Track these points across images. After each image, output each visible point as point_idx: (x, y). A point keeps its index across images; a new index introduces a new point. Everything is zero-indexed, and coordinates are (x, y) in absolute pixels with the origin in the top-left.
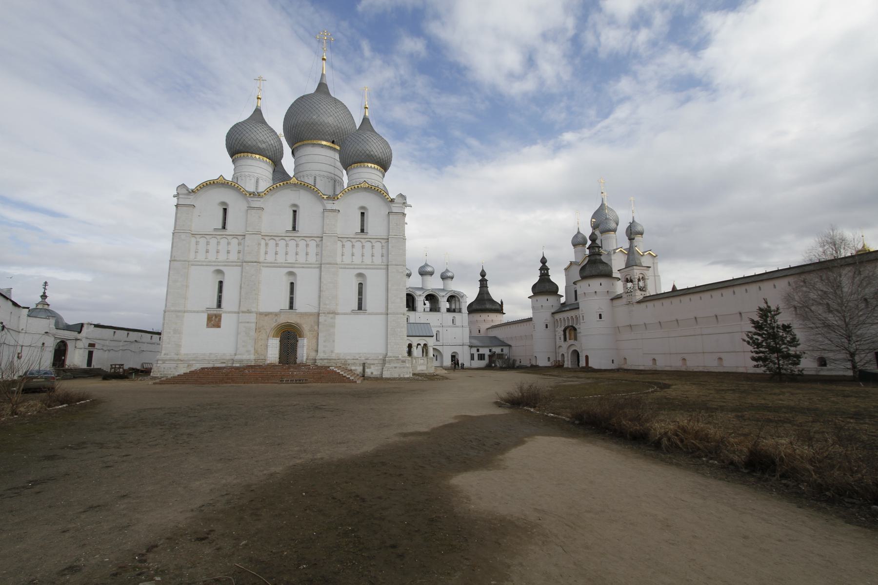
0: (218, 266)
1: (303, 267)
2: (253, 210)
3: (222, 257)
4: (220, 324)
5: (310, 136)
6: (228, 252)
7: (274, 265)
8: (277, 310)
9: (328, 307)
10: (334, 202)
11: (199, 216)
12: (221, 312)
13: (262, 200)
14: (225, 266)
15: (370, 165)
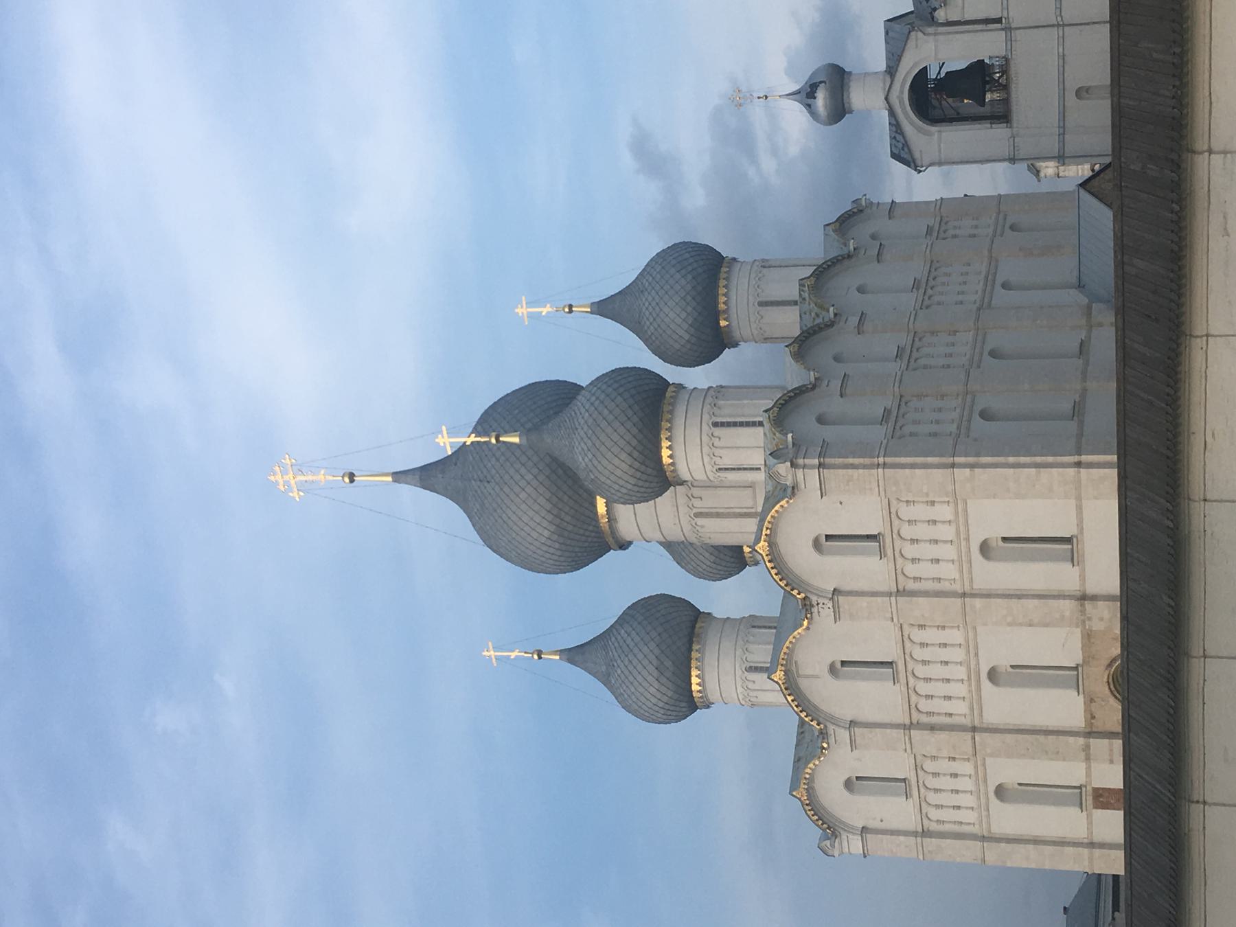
0: (987, 793)
1: (976, 654)
2: (857, 742)
3: (966, 784)
4: (1114, 789)
5: (592, 531)
6: (955, 775)
7: (977, 701)
8: (1080, 700)
9: (1067, 614)
10: (815, 603)
11: (882, 821)
12: (1089, 788)
13: (831, 727)
14: (985, 781)
15: (665, 453)
